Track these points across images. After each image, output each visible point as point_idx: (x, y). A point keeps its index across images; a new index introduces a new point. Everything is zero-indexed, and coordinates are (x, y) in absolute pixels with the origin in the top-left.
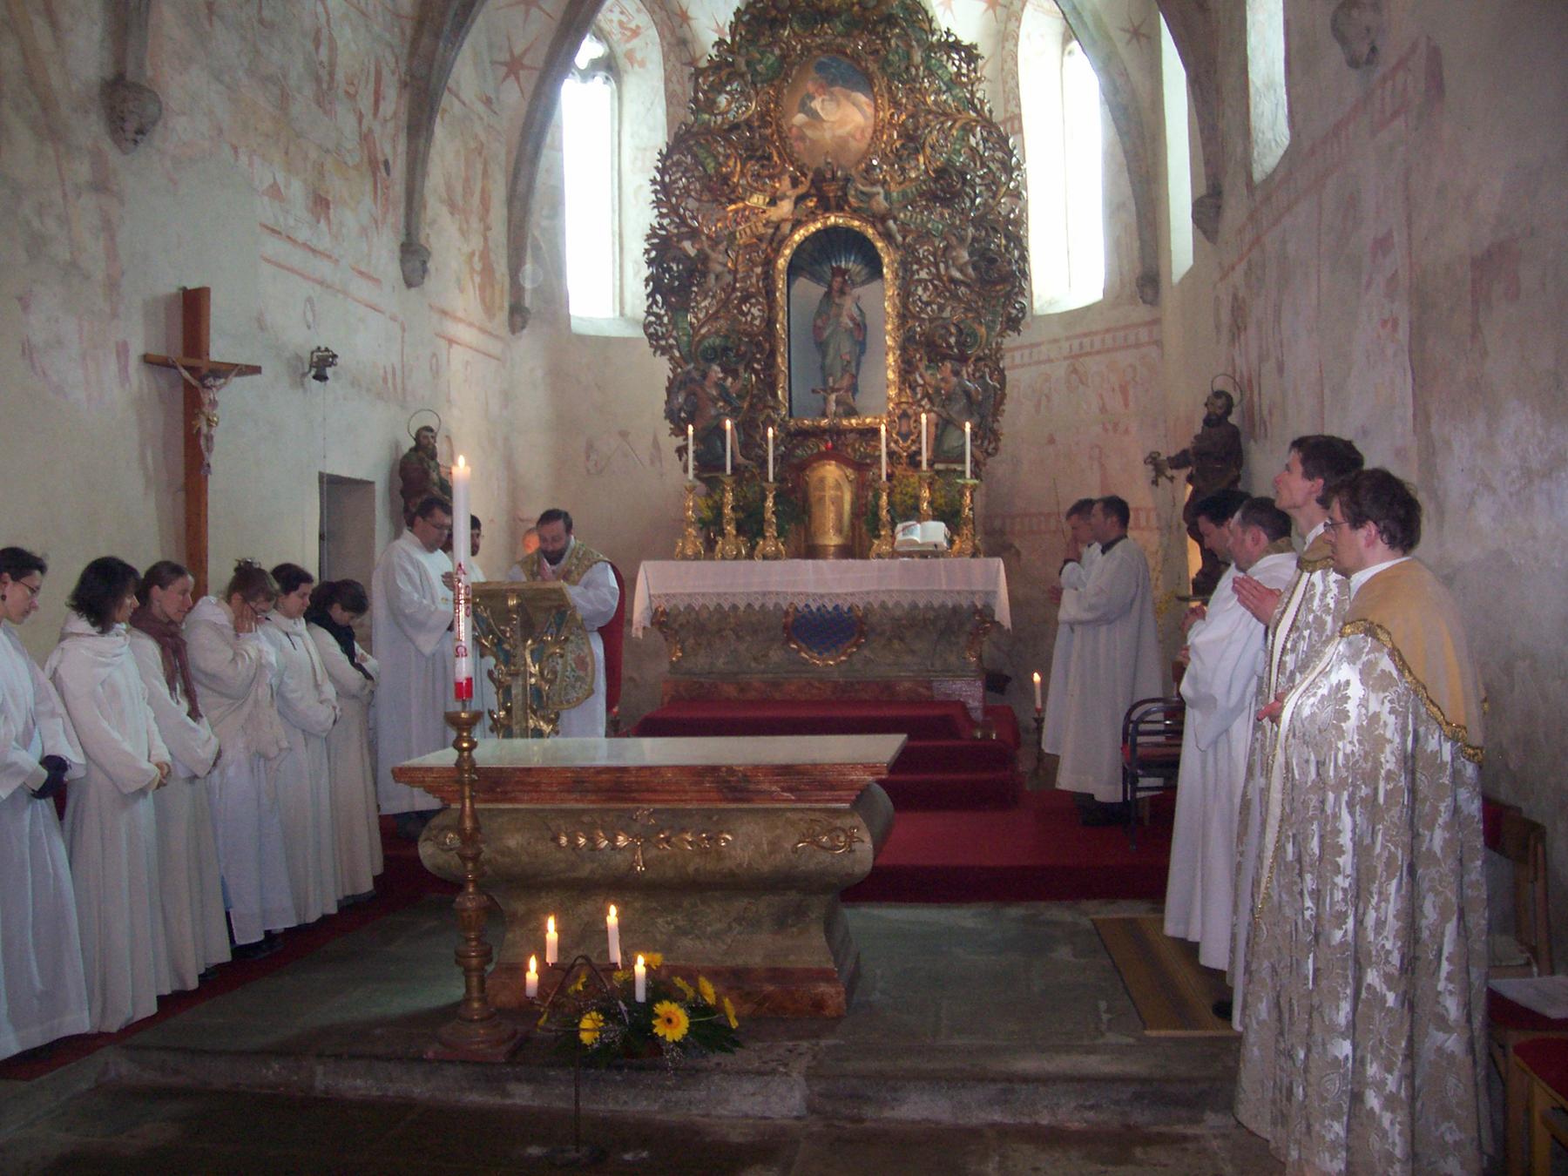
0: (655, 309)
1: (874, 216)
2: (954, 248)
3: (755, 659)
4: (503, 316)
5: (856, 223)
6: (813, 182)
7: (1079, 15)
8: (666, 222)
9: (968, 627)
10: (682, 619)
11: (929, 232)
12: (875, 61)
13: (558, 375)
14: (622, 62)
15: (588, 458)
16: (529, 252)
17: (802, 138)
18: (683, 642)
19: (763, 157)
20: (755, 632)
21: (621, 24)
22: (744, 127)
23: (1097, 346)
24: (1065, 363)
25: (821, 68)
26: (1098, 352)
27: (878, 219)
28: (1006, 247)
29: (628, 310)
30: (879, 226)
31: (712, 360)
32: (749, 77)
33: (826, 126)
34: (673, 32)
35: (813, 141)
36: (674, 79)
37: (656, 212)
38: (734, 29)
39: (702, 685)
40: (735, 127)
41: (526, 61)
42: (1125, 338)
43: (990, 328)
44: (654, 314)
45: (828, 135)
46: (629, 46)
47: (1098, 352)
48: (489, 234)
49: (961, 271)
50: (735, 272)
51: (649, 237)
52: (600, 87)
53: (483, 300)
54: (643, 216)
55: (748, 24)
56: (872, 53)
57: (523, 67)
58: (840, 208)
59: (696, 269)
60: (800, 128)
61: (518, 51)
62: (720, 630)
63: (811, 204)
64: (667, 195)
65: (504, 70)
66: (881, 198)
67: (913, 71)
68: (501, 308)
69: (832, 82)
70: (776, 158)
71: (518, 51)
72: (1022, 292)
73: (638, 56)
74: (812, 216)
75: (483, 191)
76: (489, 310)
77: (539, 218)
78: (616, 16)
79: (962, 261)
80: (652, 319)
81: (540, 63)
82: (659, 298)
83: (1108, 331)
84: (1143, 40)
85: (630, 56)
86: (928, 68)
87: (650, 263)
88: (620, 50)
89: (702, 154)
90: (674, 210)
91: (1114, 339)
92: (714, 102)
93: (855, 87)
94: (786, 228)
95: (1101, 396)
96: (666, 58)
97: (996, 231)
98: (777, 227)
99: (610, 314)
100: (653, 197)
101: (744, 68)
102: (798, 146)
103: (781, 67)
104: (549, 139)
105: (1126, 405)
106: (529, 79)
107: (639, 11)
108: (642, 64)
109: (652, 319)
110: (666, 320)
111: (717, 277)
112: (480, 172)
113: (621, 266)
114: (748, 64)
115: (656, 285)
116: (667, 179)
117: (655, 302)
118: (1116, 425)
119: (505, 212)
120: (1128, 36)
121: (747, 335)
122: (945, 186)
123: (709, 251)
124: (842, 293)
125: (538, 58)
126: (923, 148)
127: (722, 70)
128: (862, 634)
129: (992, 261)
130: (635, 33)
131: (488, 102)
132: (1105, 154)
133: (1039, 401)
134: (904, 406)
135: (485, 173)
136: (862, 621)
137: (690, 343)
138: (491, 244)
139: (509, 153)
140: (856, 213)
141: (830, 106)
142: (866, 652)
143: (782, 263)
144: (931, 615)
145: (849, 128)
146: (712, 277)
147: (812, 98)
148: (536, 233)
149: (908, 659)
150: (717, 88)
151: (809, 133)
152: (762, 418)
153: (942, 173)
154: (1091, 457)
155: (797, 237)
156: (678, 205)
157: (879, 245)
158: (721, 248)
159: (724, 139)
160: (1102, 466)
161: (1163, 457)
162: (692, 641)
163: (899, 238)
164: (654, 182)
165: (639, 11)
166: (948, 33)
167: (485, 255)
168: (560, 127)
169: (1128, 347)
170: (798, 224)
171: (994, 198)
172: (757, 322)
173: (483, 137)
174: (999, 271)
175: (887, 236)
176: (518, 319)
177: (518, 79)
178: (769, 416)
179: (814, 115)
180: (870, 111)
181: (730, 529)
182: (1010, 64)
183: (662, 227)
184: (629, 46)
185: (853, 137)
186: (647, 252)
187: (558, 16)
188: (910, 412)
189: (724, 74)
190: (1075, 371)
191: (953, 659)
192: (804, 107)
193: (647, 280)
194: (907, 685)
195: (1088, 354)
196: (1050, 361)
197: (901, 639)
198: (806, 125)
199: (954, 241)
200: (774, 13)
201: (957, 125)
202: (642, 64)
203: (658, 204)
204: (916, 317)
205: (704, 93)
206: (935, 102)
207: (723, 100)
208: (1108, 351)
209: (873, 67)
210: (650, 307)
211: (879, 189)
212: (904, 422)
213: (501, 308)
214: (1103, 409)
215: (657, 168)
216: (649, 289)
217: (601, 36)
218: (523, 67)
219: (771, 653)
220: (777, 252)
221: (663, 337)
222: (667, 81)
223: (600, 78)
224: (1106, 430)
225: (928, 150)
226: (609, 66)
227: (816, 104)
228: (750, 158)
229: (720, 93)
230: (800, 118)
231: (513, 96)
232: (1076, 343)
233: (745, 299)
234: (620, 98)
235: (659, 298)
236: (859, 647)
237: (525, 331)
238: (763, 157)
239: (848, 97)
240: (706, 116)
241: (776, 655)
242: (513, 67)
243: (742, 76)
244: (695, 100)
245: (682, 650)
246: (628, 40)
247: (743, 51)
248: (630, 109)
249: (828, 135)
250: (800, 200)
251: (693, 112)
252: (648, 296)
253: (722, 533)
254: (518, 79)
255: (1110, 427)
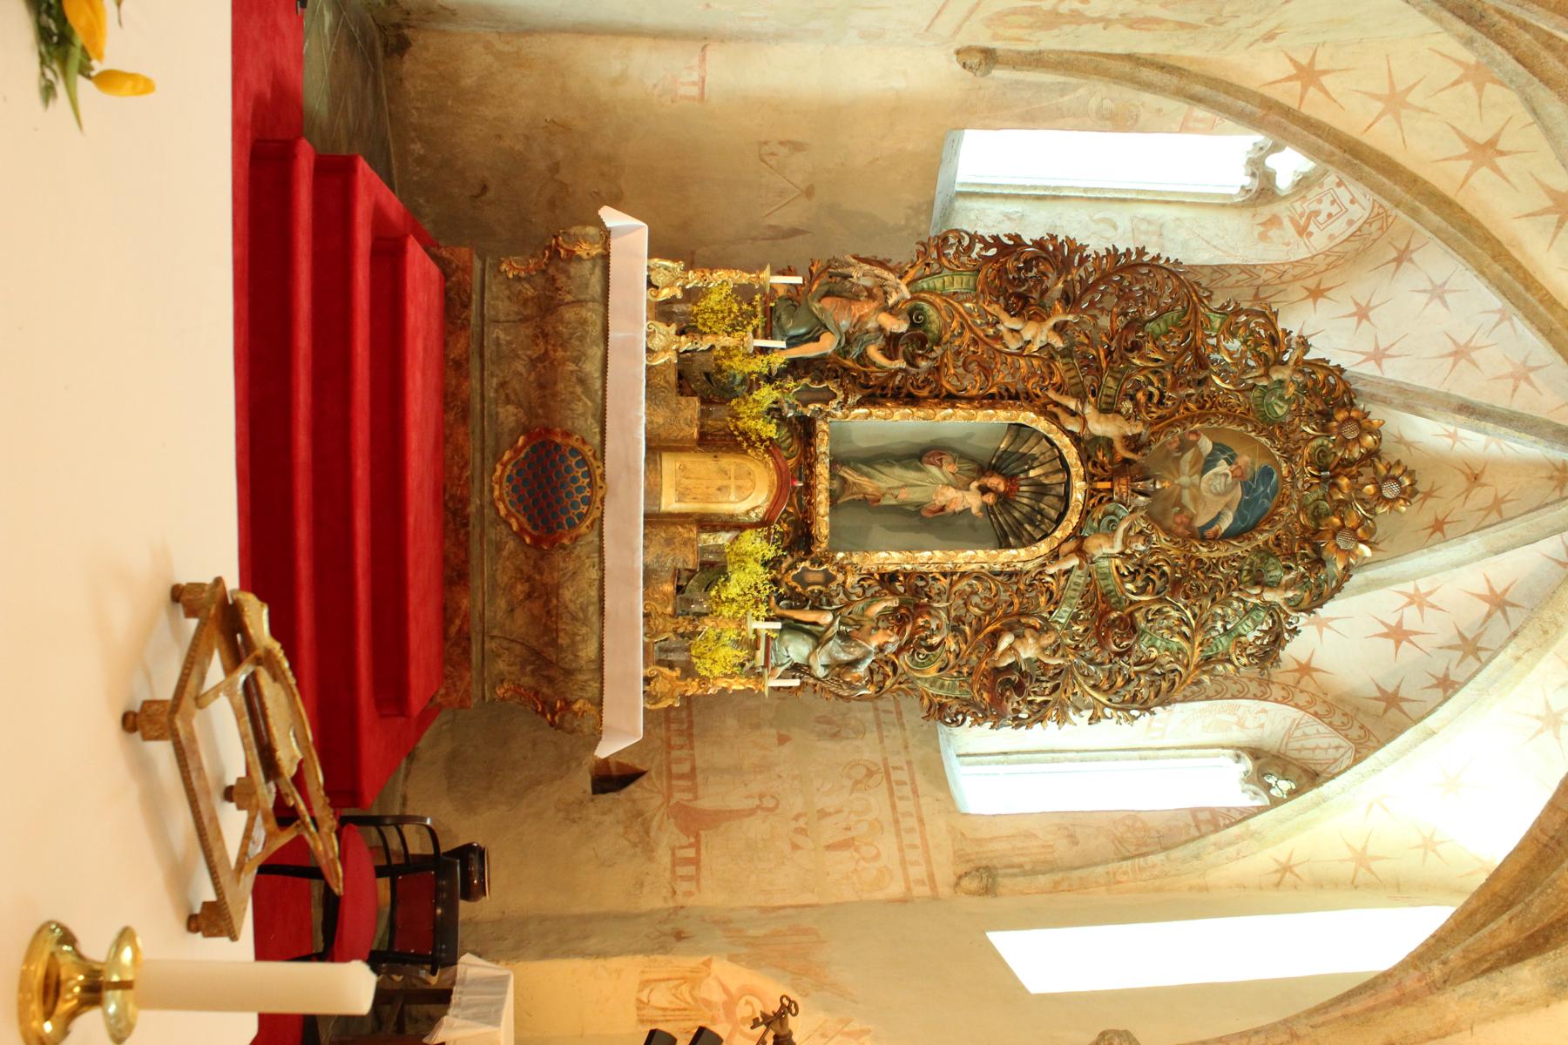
0: (979, 246)
1: (1083, 539)
2: (1037, 640)
3: (503, 385)
4: (985, 42)
5: (1075, 520)
6: (1126, 461)
7: (1317, 804)
8: (1090, 265)
9: (546, 690)
10: (562, 280)
11: (1056, 603)
12: (1266, 543)
13: (896, 110)
14: (1266, 212)
15: (781, 143)
16: (1061, 79)
17: (1184, 447)
18: (529, 279)
19: (1162, 395)
20: (542, 387)
21: (1317, 213)
22: (1203, 374)
23: (901, 805)
24: (878, 758)
25: (1267, 473)
26: (894, 807)
27: (1078, 535)
28: (1031, 702)
29: (959, 203)
30: (1072, 545)
31: (913, 325)
32: (1265, 383)
33: (1196, 477)
34: (1296, 278)
35: (1178, 459)
36: (1244, 276)
37: (1103, 253)
38: (1321, 364)
39: (466, 306)
40: (1201, 362)
41: (1312, 90)
42: (915, 847)
43: (933, 683)
44: (970, 248)
45: (1184, 480)
46: (1286, 222)
47: (894, 807)
48: (1101, 25)
49: (1011, 647)
50: (1020, 355)
51: (1070, 241)
52: (1235, 179)
53: (1015, 12)
54: (1096, 234)
55: (1326, 383)
56: (1277, 538)
57: (1305, 88)
58: (1091, 493)
59: (1023, 304)
60: (1194, 444)
61: (1326, 81)
62: (545, 336)
63: (1100, 454)
64: (1124, 268)
65: (1304, 61)
66: (1109, 551)
67: (1257, 591)
68: (995, 37)
69: (1247, 489)
70: (1160, 412)
71: (1326, 81)
72: (976, 722)
73: (1273, 233)
74: (1086, 457)
75: (1158, 21)
76: (1001, 17)
77: (1097, 93)
78: (1326, 207)
79: (1021, 650)
80: (966, 242)
81: (1306, 110)
82: (992, 252)
83: (921, 821)
84: (1276, 877)
85: (1274, 221)
86: (1255, 606)
87: (1039, 244)
88: (1279, 208)
89: (1171, 316)
90: (1105, 277)
91: (911, 830)
92: (1234, 335)
93: (1239, 515)
94: (1074, 427)
95: (839, 811)
96: (1268, 267)
97: (1056, 688)
98: (1073, 414)
99: (959, 179)
100: (1122, 250)
101: (1275, 377)
102: (1170, 439)
103: (1271, 423)
104: (1200, 112)
105: (828, 847)
106: (1287, 95)
107: (1331, 237)
108: (1263, 237)
109: (966, 242)
110: (964, 259)
111: (1012, 330)
112: (1182, 18)
113: (1017, 196)
114: (1281, 382)
115: (1009, 248)
116: (1145, 270)
117: (987, 246)
118: (801, 831)
119: (1119, 50)
120: (1283, 859)
121: (938, 369)
122: (1109, 620)
123: (1051, 322)
124: (984, 490)
125: (1316, 107)
126: (1161, 600)
127: (1272, 346)
128: (537, 542)
129: (1019, 689)
130: (1303, 231)
131: (1270, 37)
132: (1133, 816)
133: (829, 722)
134: (840, 577)
135: (1182, 25)
136: (554, 542)
137: (931, 291)
138: (1085, 27)
139: (1192, 60)
140: (1086, 513)
141: (1219, 484)
142: (511, 545)
143: (1027, 417)
144: (564, 640)
145: (1191, 507)
146: (1016, 324)
147: (1229, 464)
148: (1082, 92)
149: (502, 603)
150: (1251, 341)
151: (1189, 456)
152: (832, 386)
153: (1130, 627)
154: (761, 796)
155: (1063, 442)
156: (1108, 282)
157: (1043, 548)
158: (1058, 343)
159: (1187, 348)
160: (751, 812)
161: (793, 1023)
162: (530, 293)
163: (1052, 570)
164: (1141, 252)
165: (1331, 237)
166: (1295, 631)
167: (1076, 18)
168: (1211, 130)
169: (901, 850)
170: (1076, 439)
171: (1094, 687)
172: (954, 381)
173: (1232, 25)
174: (1006, 693)
175: (1055, 556)
176: (975, 60)
177: (1289, 79)
178: (835, 396)
179: (1209, 463)
180: (1209, 533)
181: (686, 343)
182: (1234, 688)
183: (1083, 261)
184: (1286, 222)
185: (1180, 512)
186: (1053, 238)
187: (1369, 140)
188: (833, 586)
189: (1262, 349)
190: (870, 774)
191: (501, 665)
192: (1220, 449)
193: (1016, 238)
194: (465, 603)
195: (892, 794)
196: (882, 742)
197: (529, 596)
198: (1199, 454)
199: (1048, 640)
200: (1341, 416)
201: (1184, 644)
202: (1263, 237)
203: (1113, 254)
204: (952, 585)
205: (1247, 323)
206: (1214, 615)
207: (1235, 345)
208: (897, 822)
209: (1261, 539)
210: (982, 239)
211: (1118, 548)
212: (819, 577)
213: (995, 37)
214: (823, 814)
215: (1159, 257)
216: (1005, 240)
217: (1304, 184)
218: (1305, 88)
219: (511, 408)
220: (1043, 411)
221: (941, 254)
222: (1243, 269)
223: (1254, 184)
224: (796, 818)
225: (1156, 607)
226: (1263, 192)
227: (1222, 467)
228: (1163, 381)
229: (1244, 343)
230: (1206, 445)
231: (1264, 69)
232: (903, 775)
233: (987, 371)
234: (1223, 205)
235: (992, 252)
236: (519, 535)
237: (958, 67)
238: (1162, 395)
239: (1227, 506)
240: (1217, 324)
241: (509, 415)
242: (1307, 74)
243: (1267, 375)
244: (1238, 312)
245: (518, 279)
246: (1292, 220)
247: (1299, 378)
248: (1209, 218)
249: (1184, 480)
250: (1109, 443)
251: (1223, 307)
252: (996, 238)
253: (681, 333)
254: (1289, 79)
255: (801, 823)
